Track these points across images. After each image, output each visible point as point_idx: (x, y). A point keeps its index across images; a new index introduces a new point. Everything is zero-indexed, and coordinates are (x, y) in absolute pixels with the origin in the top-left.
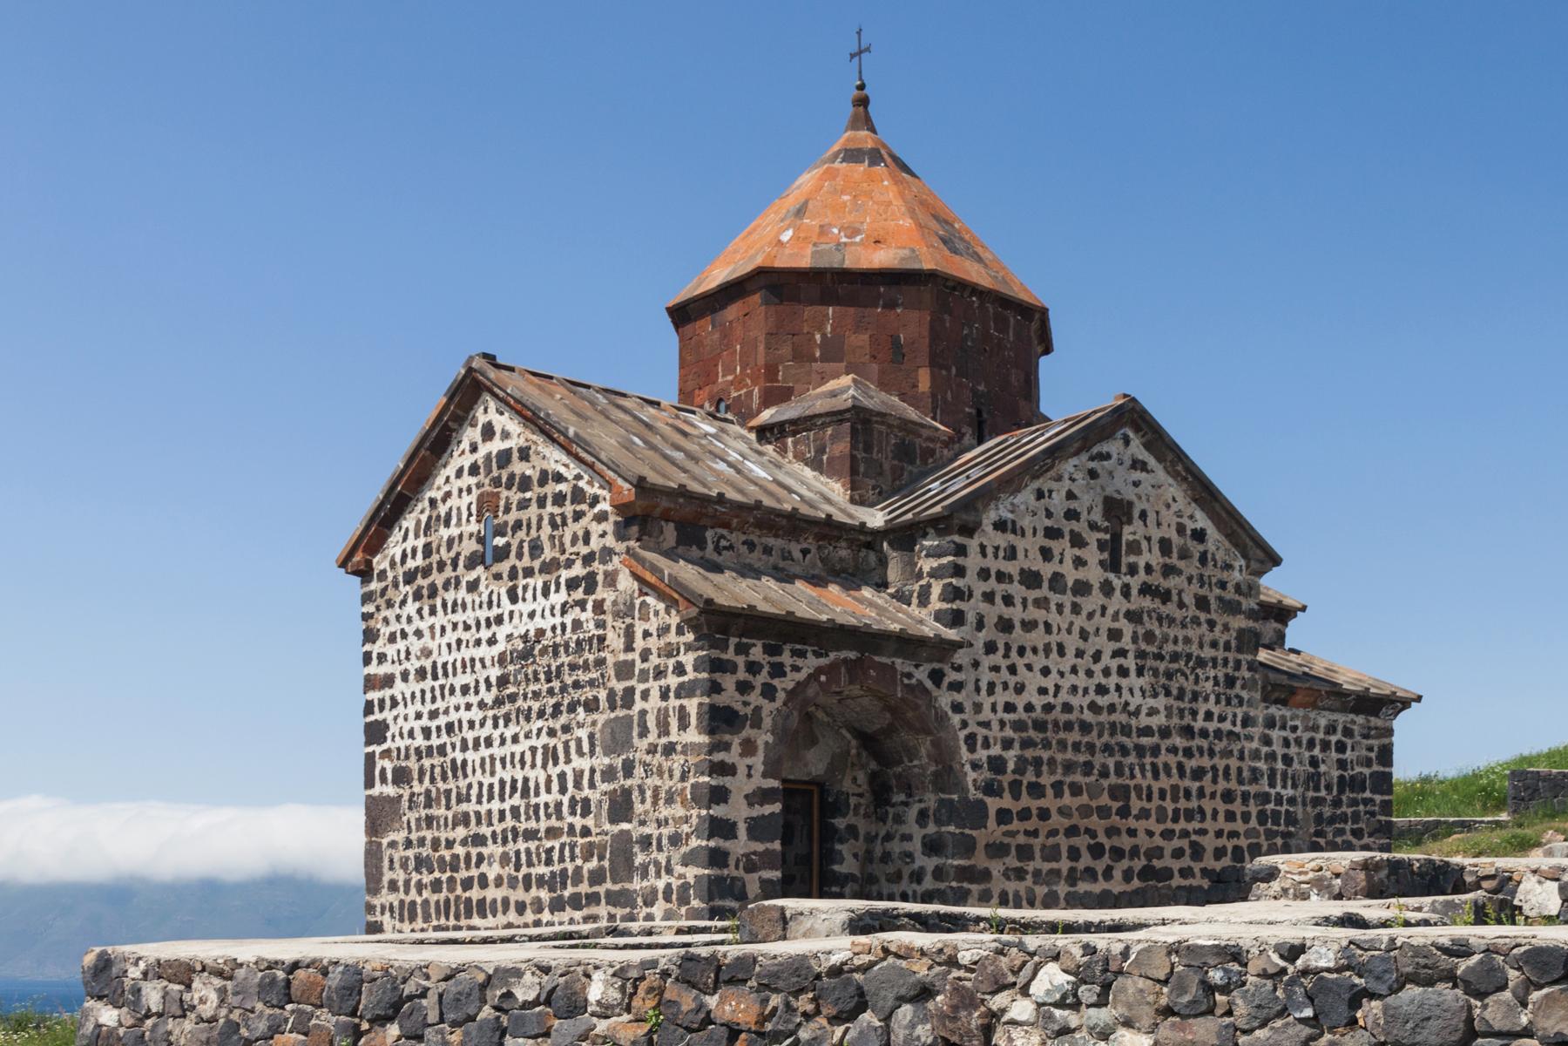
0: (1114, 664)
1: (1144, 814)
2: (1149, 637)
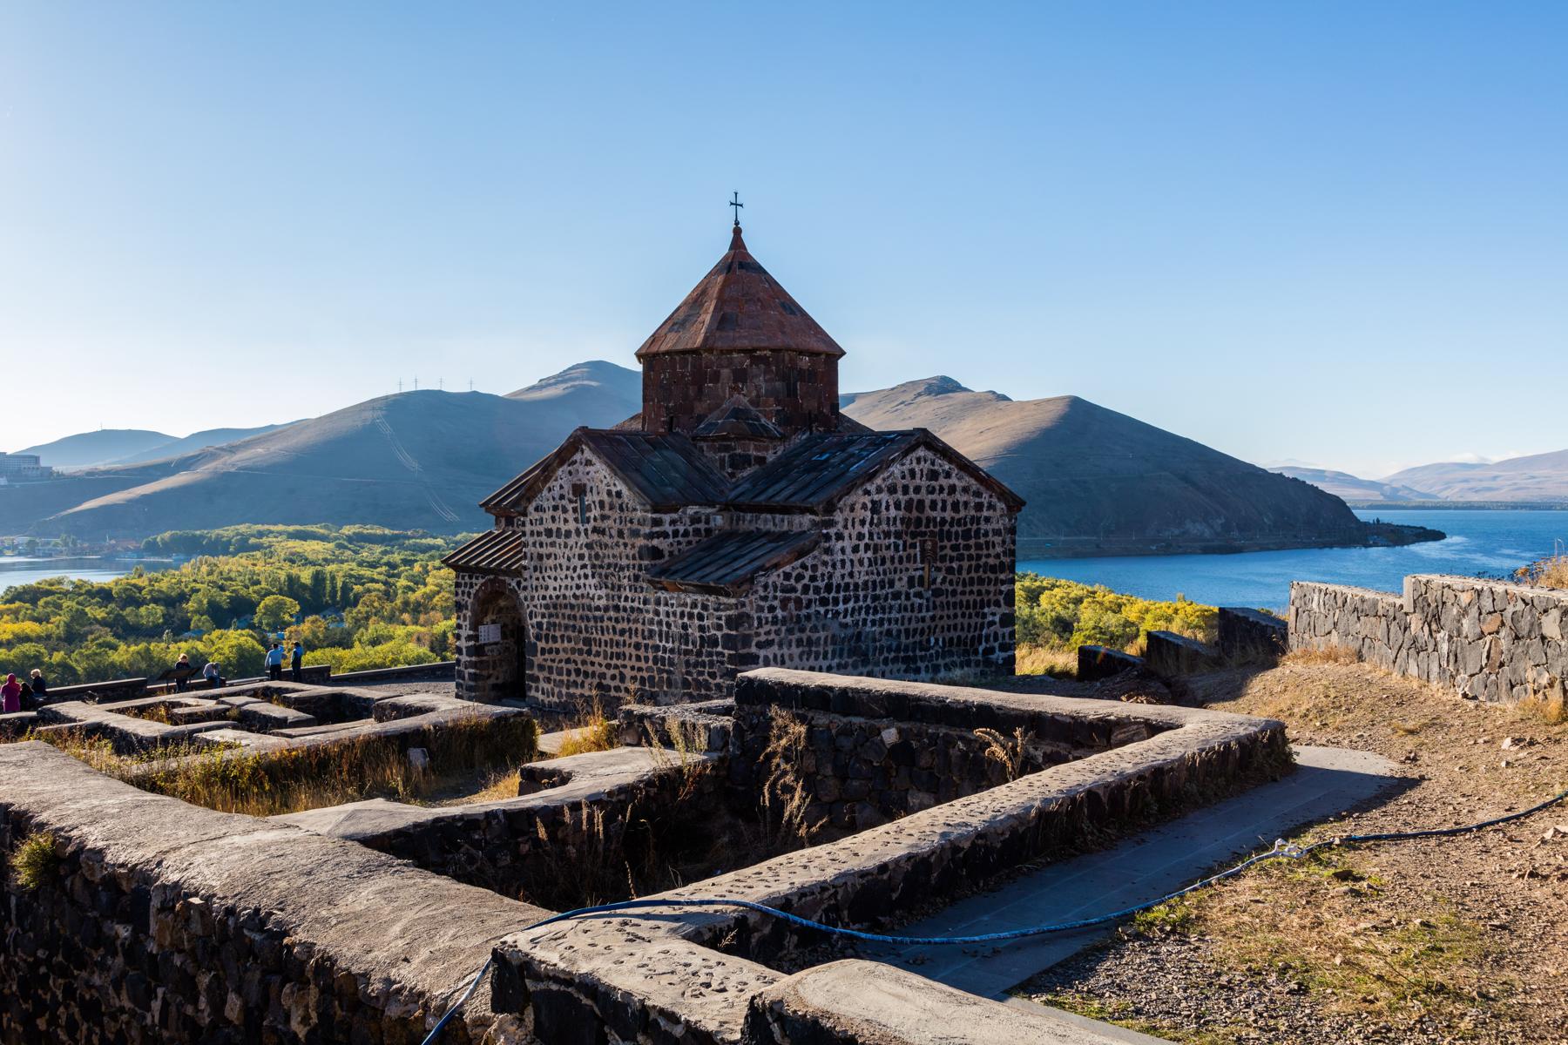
0: (582, 572)
1: (598, 654)
2: (597, 556)
